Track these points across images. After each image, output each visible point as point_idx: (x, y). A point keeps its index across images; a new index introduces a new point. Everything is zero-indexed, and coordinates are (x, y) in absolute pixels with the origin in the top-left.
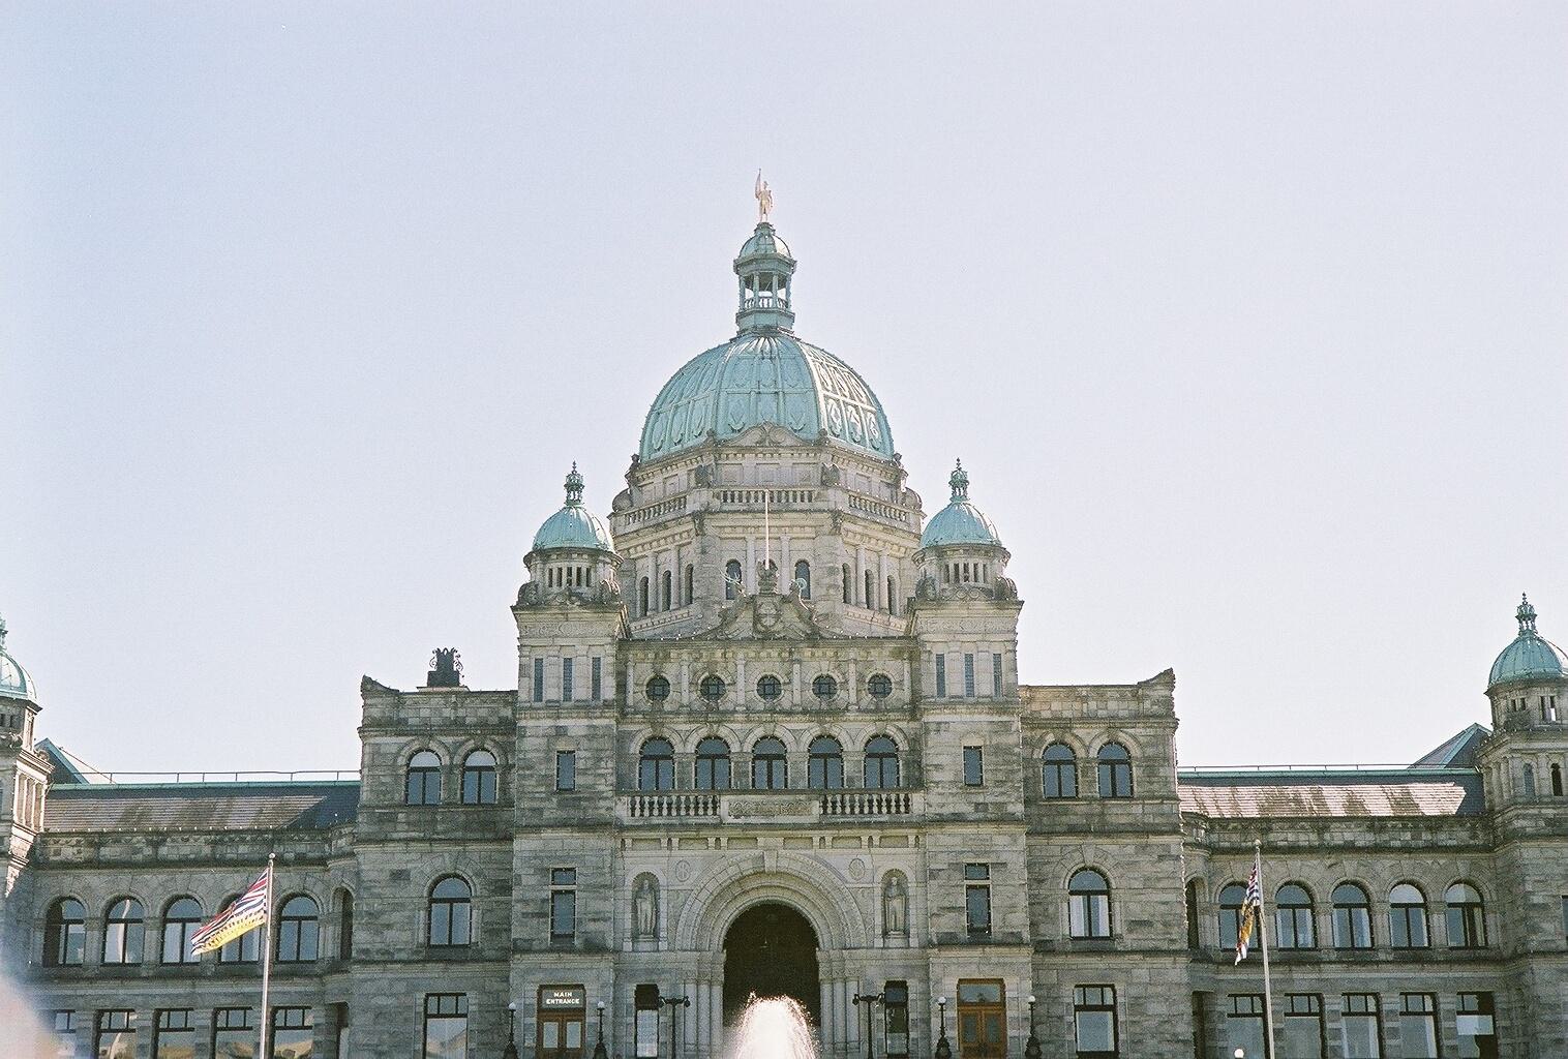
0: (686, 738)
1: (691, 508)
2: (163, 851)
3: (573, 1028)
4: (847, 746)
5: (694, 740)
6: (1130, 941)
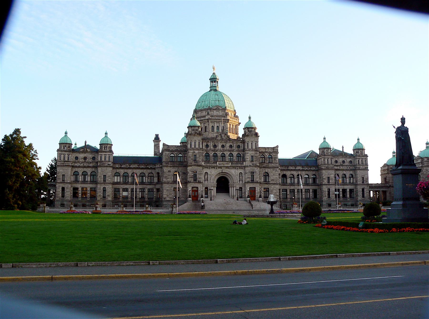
0: (211, 154)
1: (207, 118)
2: (131, 166)
3: (196, 193)
4: (234, 155)
5: (212, 154)
6: (271, 182)
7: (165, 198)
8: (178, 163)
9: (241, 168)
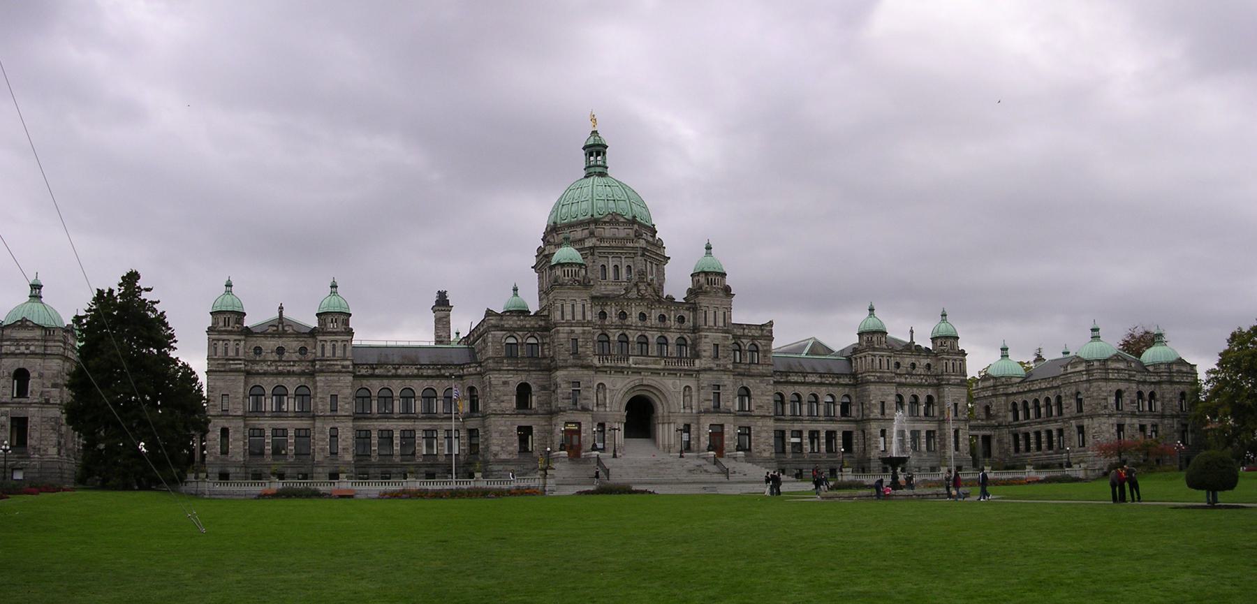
4: (670, 341)
6: (757, 412)
7: (496, 455)
8: (527, 361)
9: (688, 373)
